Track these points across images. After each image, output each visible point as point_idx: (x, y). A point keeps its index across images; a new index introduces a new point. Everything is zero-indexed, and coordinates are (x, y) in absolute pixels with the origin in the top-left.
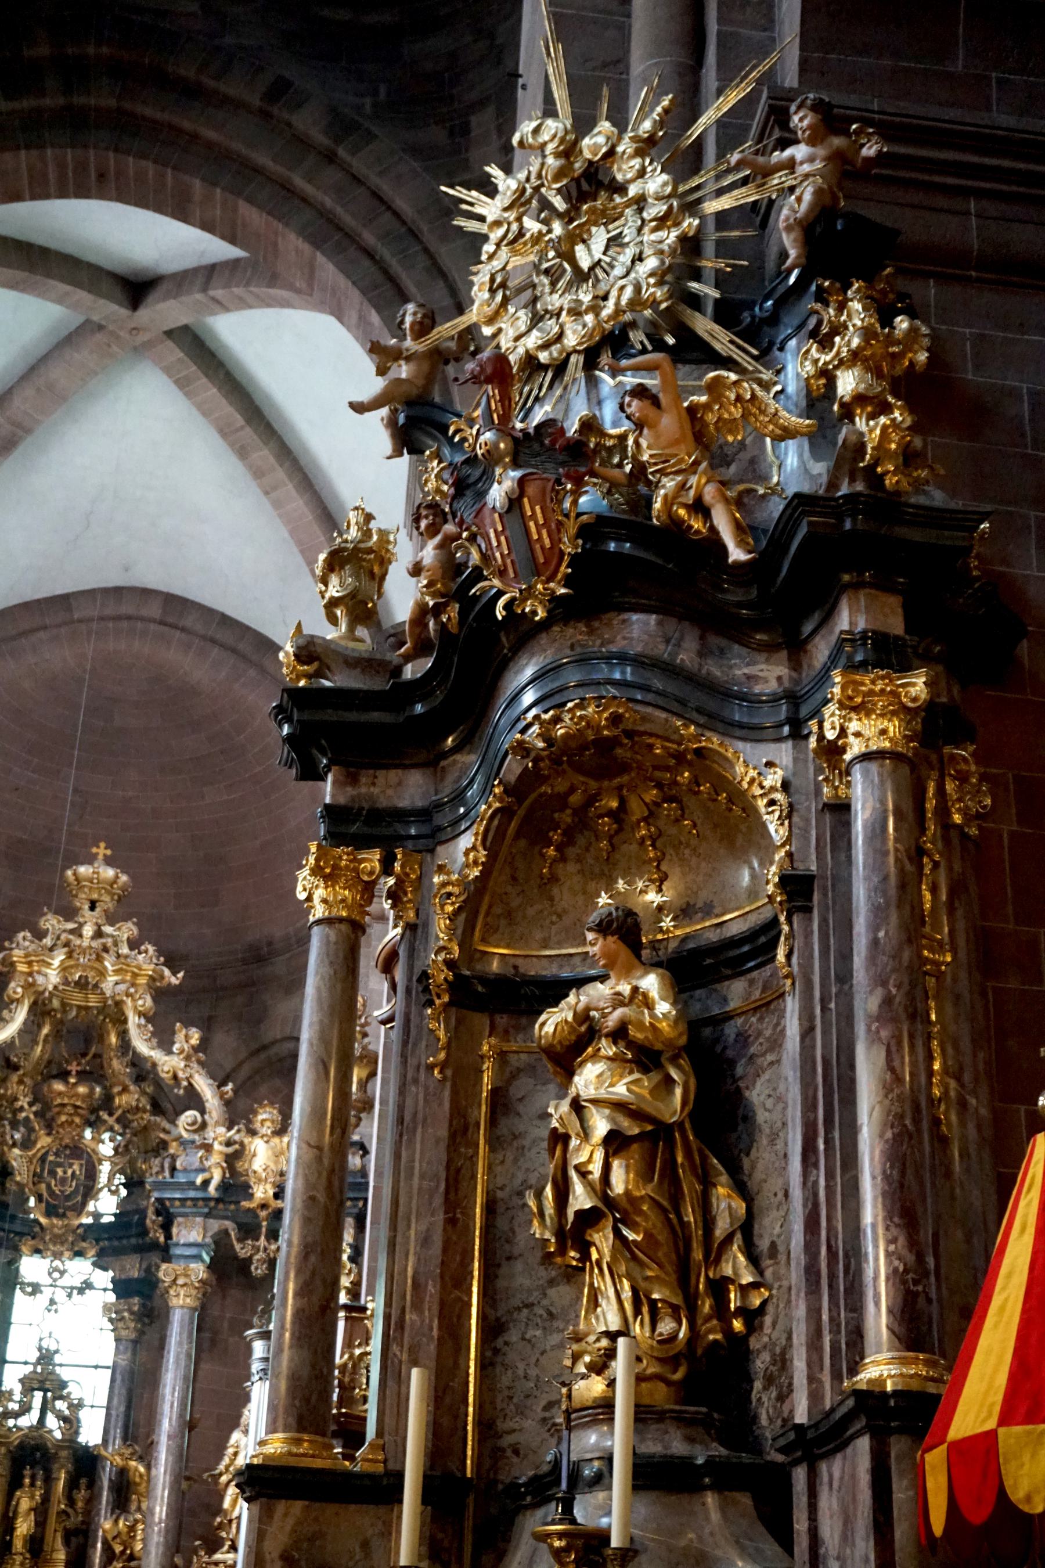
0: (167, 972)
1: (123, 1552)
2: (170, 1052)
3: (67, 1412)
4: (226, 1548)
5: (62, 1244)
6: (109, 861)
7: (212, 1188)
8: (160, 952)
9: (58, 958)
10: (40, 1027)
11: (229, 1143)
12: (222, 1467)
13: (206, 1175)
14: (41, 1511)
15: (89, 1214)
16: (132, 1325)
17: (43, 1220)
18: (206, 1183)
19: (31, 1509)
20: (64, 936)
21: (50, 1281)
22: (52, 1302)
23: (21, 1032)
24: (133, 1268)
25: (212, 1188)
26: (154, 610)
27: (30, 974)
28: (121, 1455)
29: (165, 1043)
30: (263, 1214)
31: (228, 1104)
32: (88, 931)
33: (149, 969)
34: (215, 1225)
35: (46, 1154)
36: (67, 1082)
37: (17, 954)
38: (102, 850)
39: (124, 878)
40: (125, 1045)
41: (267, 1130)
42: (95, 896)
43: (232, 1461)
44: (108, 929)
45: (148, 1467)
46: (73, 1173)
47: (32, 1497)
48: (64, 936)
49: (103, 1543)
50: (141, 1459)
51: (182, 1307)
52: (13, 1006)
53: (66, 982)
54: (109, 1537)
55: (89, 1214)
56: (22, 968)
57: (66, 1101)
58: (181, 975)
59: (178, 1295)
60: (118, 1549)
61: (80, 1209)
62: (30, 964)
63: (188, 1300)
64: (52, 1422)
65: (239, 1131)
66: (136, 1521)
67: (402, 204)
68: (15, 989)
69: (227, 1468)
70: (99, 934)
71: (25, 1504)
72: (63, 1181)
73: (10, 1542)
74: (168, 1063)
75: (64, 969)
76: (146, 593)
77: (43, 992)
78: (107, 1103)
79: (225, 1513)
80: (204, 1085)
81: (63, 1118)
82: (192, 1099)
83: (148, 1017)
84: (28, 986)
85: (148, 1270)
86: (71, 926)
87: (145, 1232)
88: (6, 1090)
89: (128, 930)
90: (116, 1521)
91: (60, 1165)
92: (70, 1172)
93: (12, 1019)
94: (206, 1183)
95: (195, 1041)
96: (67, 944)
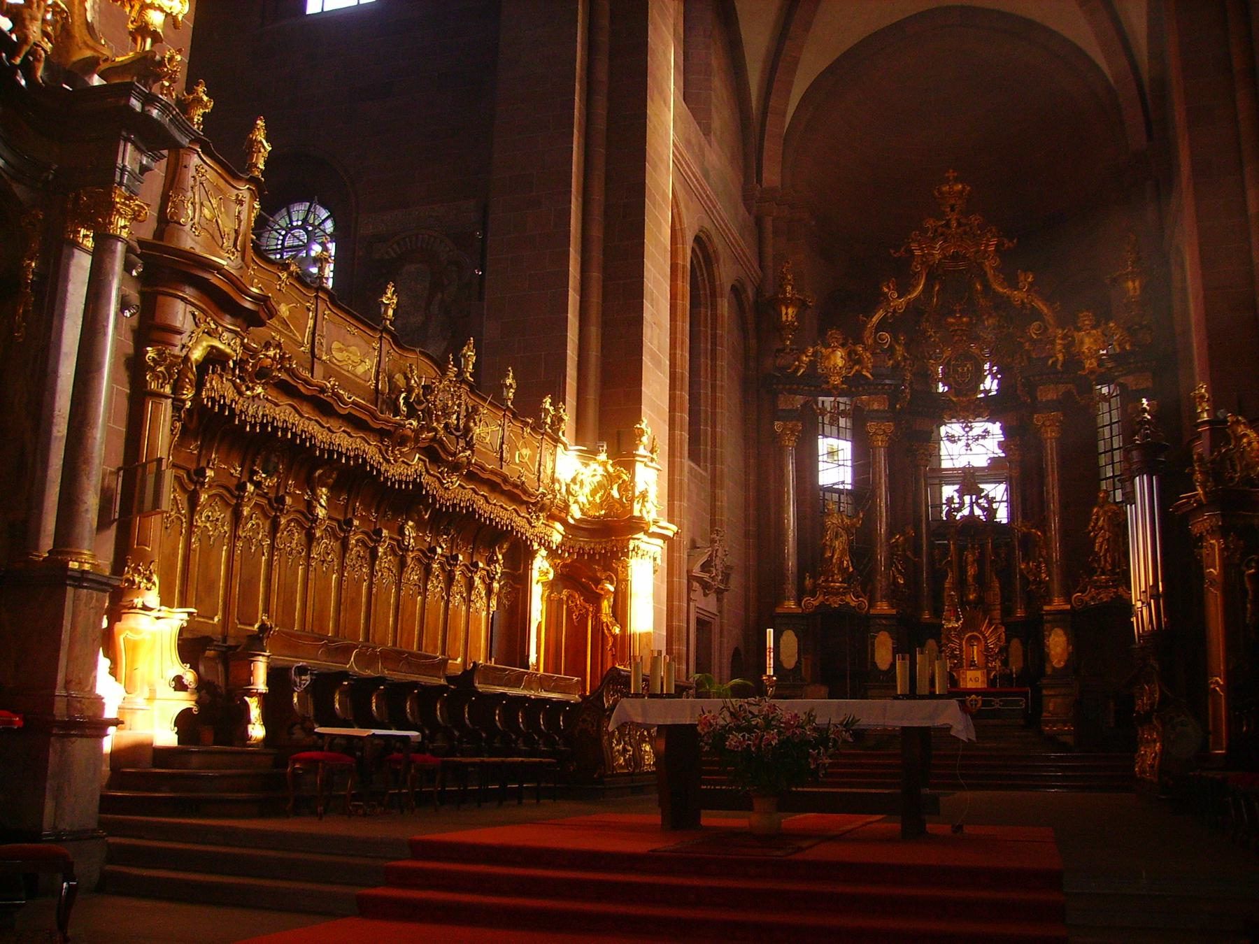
0: (1006, 241)
1: (1035, 580)
2: (1017, 289)
3: (986, 505)
4: (1098, 573)
5: (967, 411)
6: (957, 180)
7: (1059, 367)
10: (933, 287)
13: (1054, 359)
14: (980, 561)
15: (982, 392)
16: (1017, 453)
18: (1055, 363)
19: (974, 560)
20: (940, 230)
21: (964, 433)
22: (968, 445)
23: (923, 291)
25: (1059, 367)
27: (923, 256)
28: (1025, 526)
29: (1014, 285)
30: (1093, 377)
33: (994, 242)
34: (1062, 388)
35: (950, 360)
36: (955, 317)
37: (914, 246)
38: (951, 174)
40: (987, 287)
42: (953, 202)
43: (1096, 524)
44: (963, 221)
45: (1044, 532)
46: (968, 368)
47: (974, 555)
48: (940, 230)
49: (1020, 576)
50: (1038, 528)
51: (1051, 439)
52: (917, 277)
53: (945, 257)
54: (1025, 572)
55: (982, 392)
56: (918, 253)
57: (956, 328)
58: (1015, 241)
59: (1047, 432)
60: (1031, 578)
62: (922, 249)
63: (1053, 434)
64: (978, 512)
65: (1069, 330)
66: (1040, 563)
69: (1093, 527)
70: (959, 225)
71: (970, 558)
72: (962, 374)
73: (966, 580)
74: (1017, 296)
77: (932, 266)
79: (1097, 553)
80: (1040, 305)
81: (956, 338)
88: (920, 327)
89: (975, 219)
90: (1028, 564)
91: (959, 366)
92: (966, 369)
93: (918, 284)
94: (1055, 363)
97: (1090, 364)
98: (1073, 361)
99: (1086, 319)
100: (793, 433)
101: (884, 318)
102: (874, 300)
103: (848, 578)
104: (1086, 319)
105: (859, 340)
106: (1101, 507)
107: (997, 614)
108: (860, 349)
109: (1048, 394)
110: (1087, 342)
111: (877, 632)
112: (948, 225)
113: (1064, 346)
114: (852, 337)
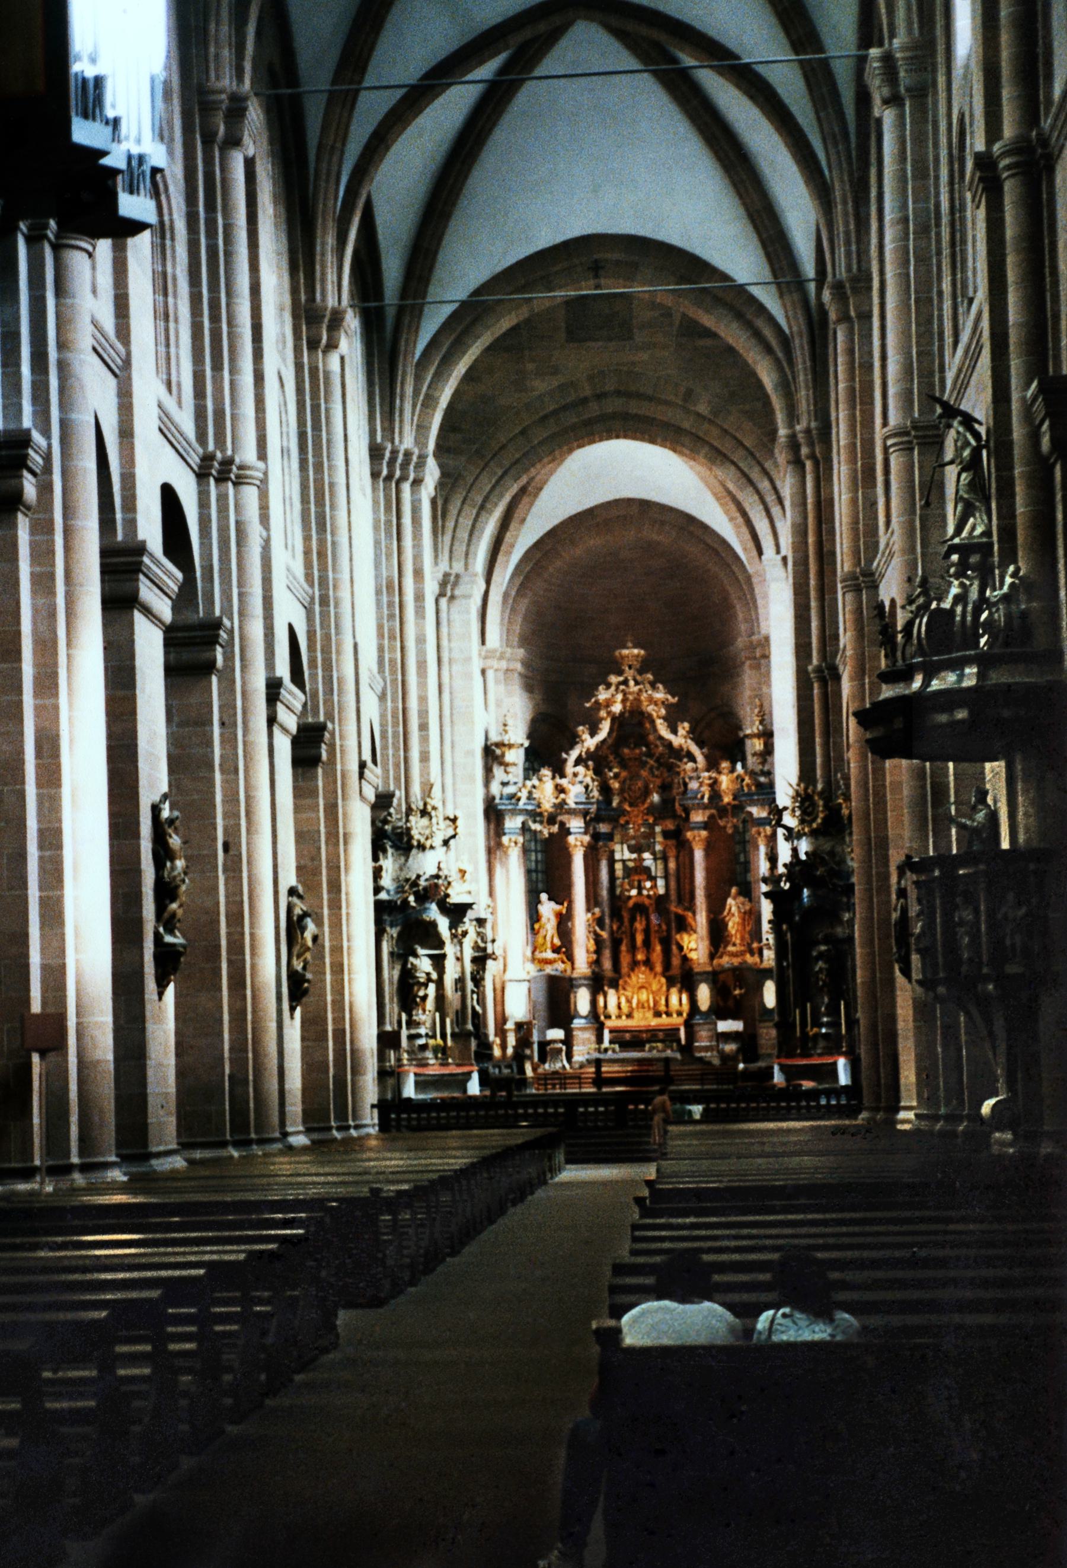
0: (669, 697)
7: (706, 800)
8: (665, 688)
9: (620, 697)
11: (710, 778)
12: (725, 913)
14: (647, 931)
17: (628, 809)
24: (670, 825)
26: (635, 510)
29: (675, 732)
31: (707, 757)
32: (632, 683)
34: (708, 813)
39: (642, 652)
41: (725, 771)
44: (638, 678)
61: (643, 802)
67: (747, 444)
68: (603, 713)
75: (624, 701)
76: (629, 501)
78: (649, 754)
82: (692, 758)
83: (665, 719)
84: (609, 713)
85: (678, 826)
86: (621, 679)
87: (675, 811)
94: (703, 797)
95: (687, 729)
96: (623, 691)
97: (727, 799)
98: (716, 794)
99: (725, 765)
100: (516, 843)
101: (580, 755)
102: (573, 740)
103: (556, 950)
104: (725, 765)
105: (563, 776)
106: (734, 898)
107: (659, 968)
108: (564, 782)
109: (698, 817)
110: (725, 782)
111: (580, 986)
112: (625, 682)
113: (711, 786)
114: (559, 770)
